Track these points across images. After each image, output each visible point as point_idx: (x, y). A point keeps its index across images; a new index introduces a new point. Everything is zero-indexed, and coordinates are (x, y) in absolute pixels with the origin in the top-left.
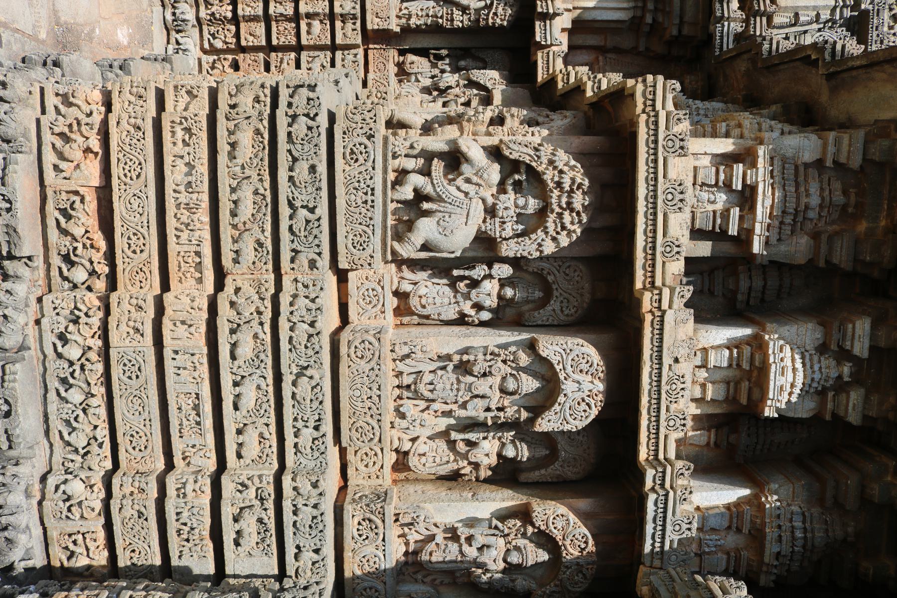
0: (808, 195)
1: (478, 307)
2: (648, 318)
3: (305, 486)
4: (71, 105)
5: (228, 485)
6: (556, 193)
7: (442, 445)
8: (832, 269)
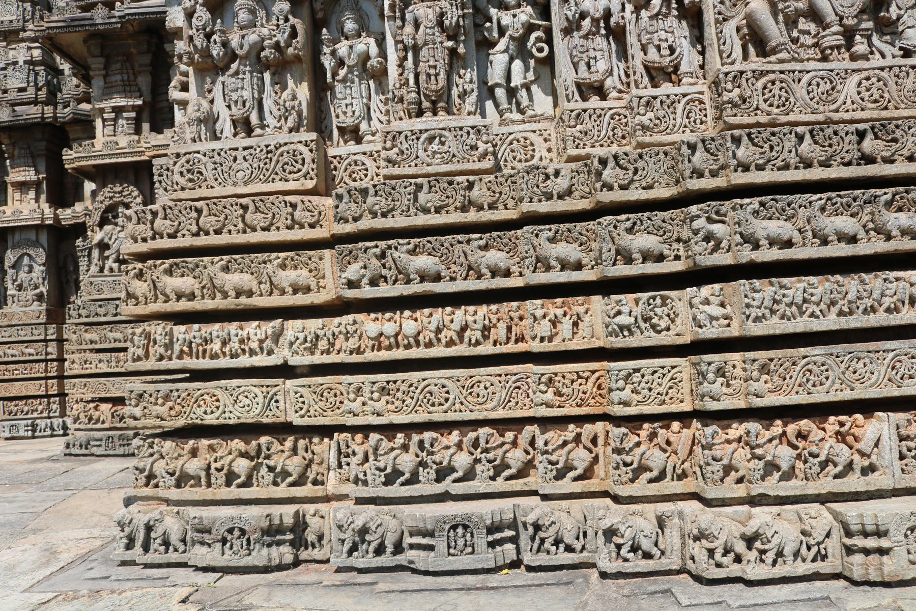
0: (116, 81)
4: (78, 418)
6: (115, 199)
8: (152, 64)
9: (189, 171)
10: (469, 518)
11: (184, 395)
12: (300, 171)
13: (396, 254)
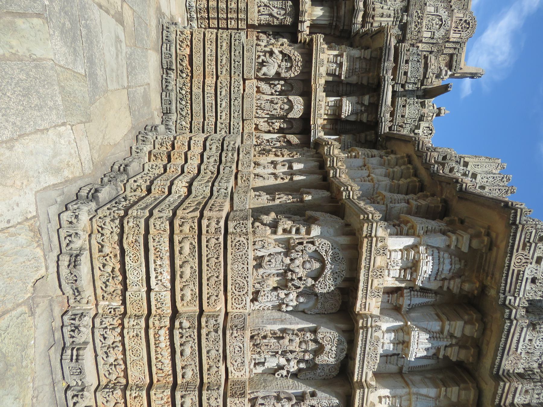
1: (276, 91)
2: (313, 90)
3: (236, 124)
5: (218, 124)
7: (266, 124)
9: (240, 244)
10: (83, 374)
11: (137, 248)
12: (236, 290)
13: (191, 342)
